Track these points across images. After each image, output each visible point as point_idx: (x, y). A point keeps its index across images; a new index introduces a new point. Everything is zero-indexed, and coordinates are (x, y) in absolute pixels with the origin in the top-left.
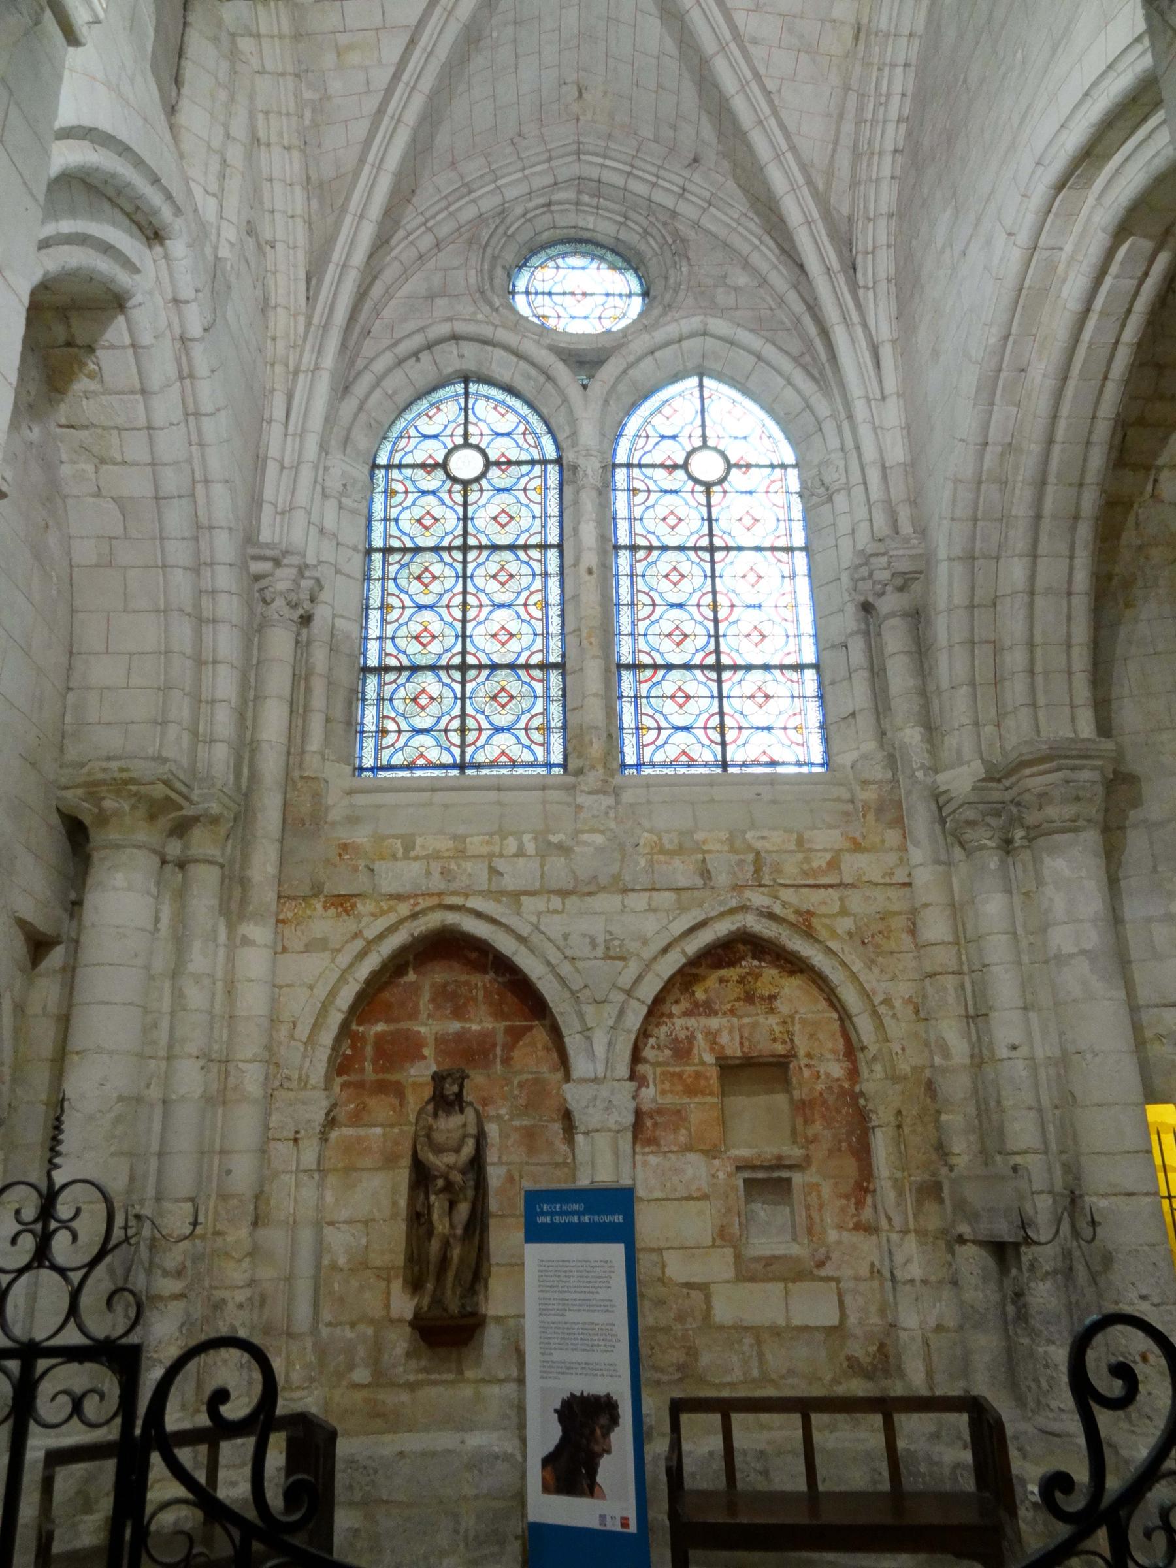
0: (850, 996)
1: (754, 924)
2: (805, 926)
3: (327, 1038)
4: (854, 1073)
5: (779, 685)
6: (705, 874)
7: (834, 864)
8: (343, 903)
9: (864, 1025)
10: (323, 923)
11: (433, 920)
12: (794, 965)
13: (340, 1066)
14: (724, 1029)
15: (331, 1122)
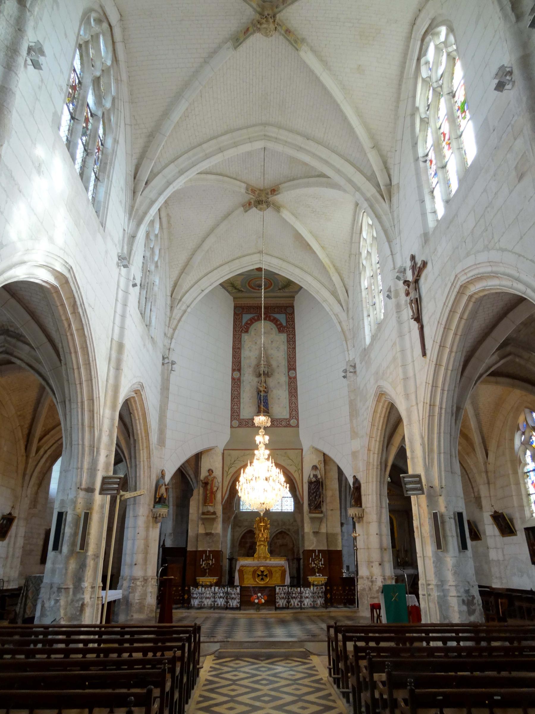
0: (293, 539)
1: (283, 530)
2: (289, 530)
3: (238, 541)
4: (294, 547)
5: (289, 499)
6: (278, 524)
7: (292, 523)
8: (240, 527)
9: (294, 542)
10: (238, 529)
11: (248, 529)
12: (288, 535)
13: (240, 544)
14: (280, 542)
15: (239, 550)
